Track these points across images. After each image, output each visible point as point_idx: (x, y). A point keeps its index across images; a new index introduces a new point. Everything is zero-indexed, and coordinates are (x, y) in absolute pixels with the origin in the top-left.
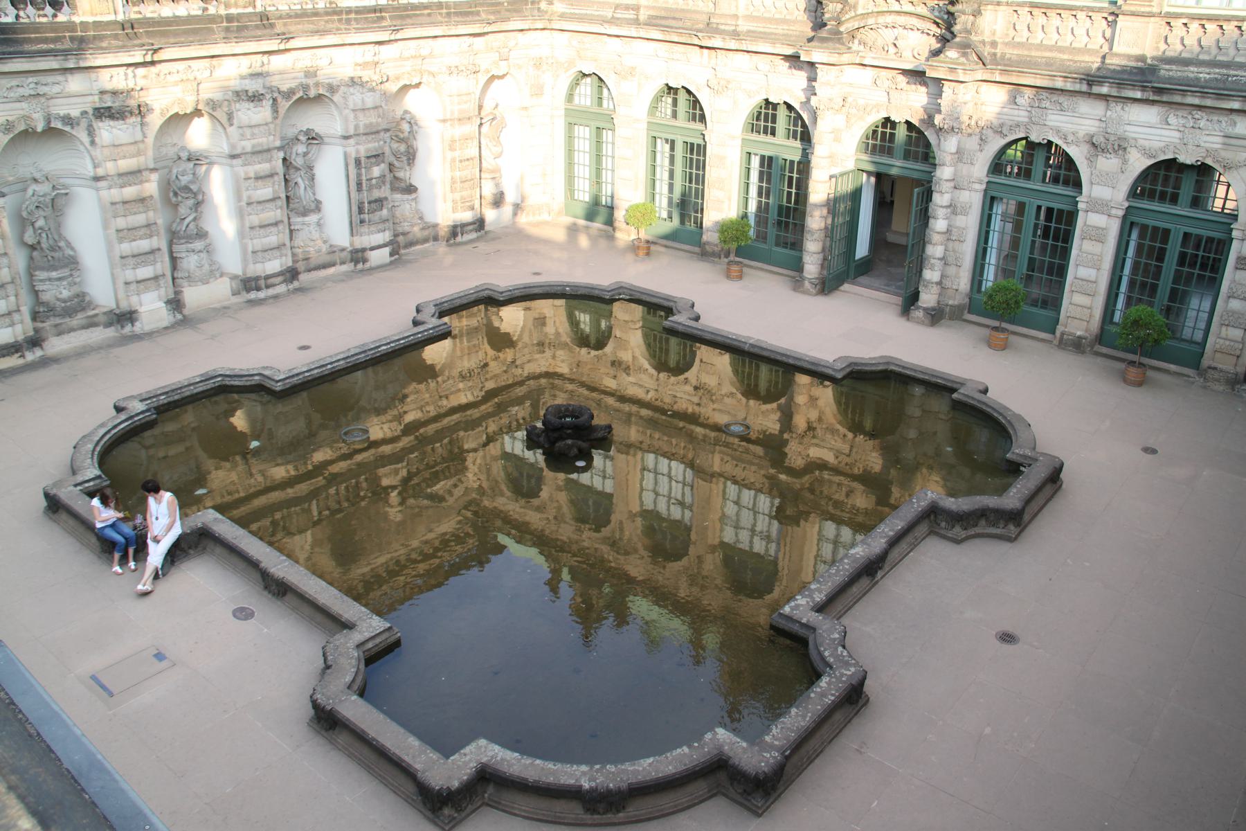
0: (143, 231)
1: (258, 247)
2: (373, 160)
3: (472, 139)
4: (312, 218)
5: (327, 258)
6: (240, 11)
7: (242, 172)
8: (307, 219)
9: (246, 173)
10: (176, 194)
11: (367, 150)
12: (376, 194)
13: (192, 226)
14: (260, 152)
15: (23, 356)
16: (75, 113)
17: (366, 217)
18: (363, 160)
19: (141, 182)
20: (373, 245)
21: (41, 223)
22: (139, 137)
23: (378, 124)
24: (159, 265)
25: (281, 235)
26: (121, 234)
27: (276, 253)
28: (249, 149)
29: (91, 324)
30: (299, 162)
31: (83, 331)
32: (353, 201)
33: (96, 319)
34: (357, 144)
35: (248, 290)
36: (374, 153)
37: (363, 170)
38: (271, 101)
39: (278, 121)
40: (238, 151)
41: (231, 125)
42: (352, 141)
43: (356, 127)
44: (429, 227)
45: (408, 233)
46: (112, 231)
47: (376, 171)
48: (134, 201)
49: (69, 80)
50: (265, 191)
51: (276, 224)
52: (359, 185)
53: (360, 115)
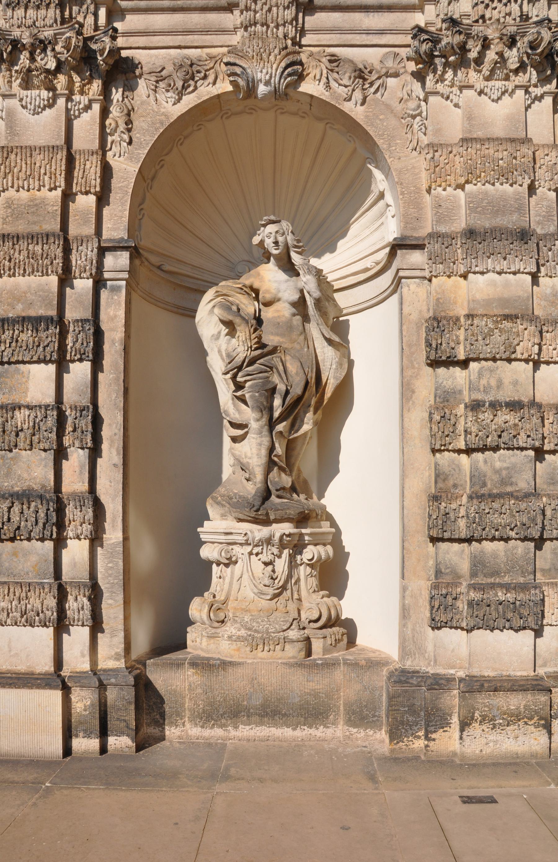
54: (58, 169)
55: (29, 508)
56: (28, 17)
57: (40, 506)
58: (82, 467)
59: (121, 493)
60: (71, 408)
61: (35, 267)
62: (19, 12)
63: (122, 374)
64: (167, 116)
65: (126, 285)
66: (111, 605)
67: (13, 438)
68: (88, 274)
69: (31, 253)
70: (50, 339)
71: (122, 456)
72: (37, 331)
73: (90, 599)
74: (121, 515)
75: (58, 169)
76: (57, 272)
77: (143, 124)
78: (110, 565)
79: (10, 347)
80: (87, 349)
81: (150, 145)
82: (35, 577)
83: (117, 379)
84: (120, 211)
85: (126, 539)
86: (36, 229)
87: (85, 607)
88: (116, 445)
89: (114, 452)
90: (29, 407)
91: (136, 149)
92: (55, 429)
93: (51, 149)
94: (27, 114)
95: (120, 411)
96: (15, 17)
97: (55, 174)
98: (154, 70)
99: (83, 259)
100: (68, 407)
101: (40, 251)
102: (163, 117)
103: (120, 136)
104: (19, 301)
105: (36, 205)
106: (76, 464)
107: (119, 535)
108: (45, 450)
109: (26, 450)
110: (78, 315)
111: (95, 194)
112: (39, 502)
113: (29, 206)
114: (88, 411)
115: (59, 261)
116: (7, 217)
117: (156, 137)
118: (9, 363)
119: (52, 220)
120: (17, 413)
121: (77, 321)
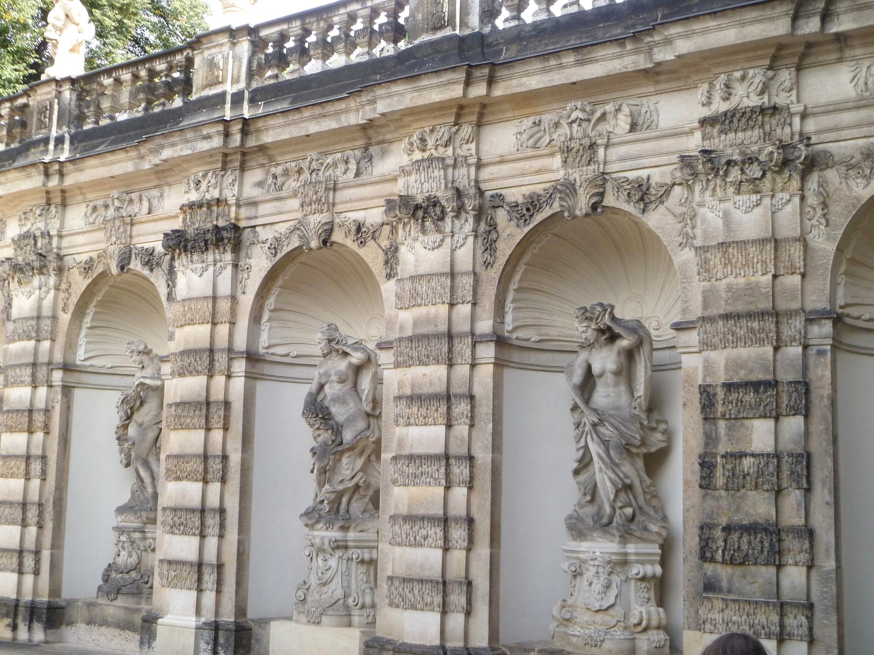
2: (750, 397)
6: (425, 38)
11: (733, 365)
14: (427, 337)
18: (721, 393)
34: (706, 345)
41: (389, 276)
43: (708, 298)
48: (190, 403)
49: (165, 195)
54: (768, 258)
55: (755, 538)
56: (737, 138)
57: (765, 537)
58: (799, 504)
59: (833, 527)
60: (788, 455)
61: (754, 340)
62: (730, 135)
63: (831, 426)
64: (858, 200)
65: (831, 349)
66: (826, 624)
67: (741, 481)
68: (798, 343)
69: (749, 328)
70: (769, 400)
71: (833, 496)
72: (758, 392)
73: (807, 617)
74: (834, 546)
75: (768, 258)
76: (772, 344)
77: (837, 208)
78: (825, 589)
79: (736, 406)
80: (800, 406)
81: (845, 226)
82: (761, 597)
83: (827, 429)
84: (822, 285)
85: (839, 567)
86: (752, 308)
87: (804, 625)
88: (828, 486)
89: (826, 492)
90: (753, 455)
91: (833, 230)
92: (776, 473)
93: (761, 242)
94: (740, 213)
95: (830, 457)
96: (728, 140)
97: (766, 263)
98: (845, 160)
99: (793, 331)
100: (785, 454)
101: (757, 326)
102: (854, 201)
103: (818, 221)
104: (741, 368)
105: (751, 288)
106: (794, 502)
107: (831, 564)
108: (767, 491)
109: (751, 490)
110: (791, 377)
111: (800, 274)
112: (764, 534)
113: (746, 289)
114: (803, 458)
115: (773, 335)
116: (729, 299)
117: (850, 218)
118: (736, 419)
119: (766, 300)
120: (744, 460)
121: (791, 383)
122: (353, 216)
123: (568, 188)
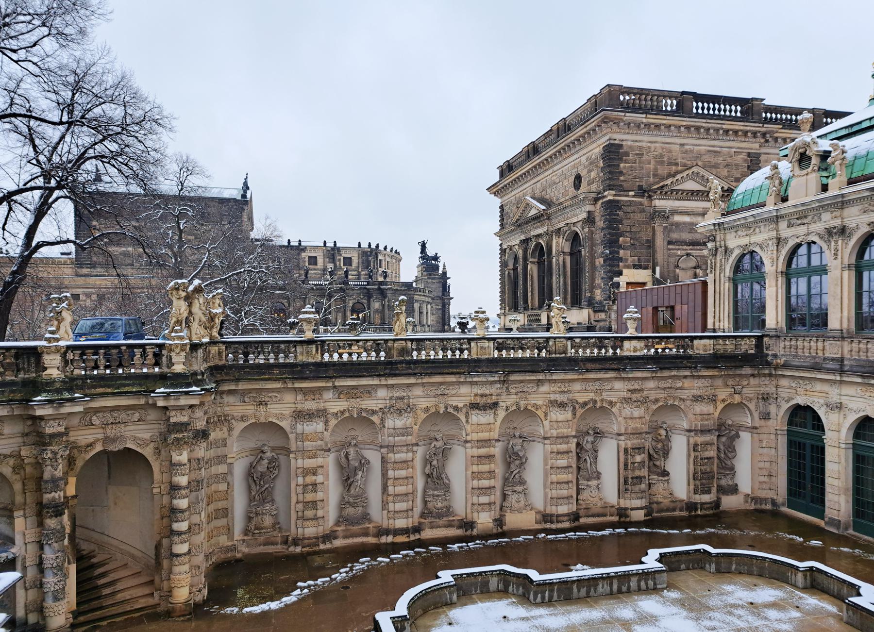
0: (486, 475)
1: (555, 495)
2: (637, 451)
3: (712, 444)
4: (594, 483)
5: (601, 511)
7: (548, 447)
8: (590, 483)
9: (552, 449)
10: (510, 457)
11: (633, 444)
12: (637, 473)
13: (517, 476)
15: (409, 537)
16: (460, 405)
17: (630, 487)
18: (629, 450)
19: (490, 447)
20: (633, 506)
21: (435, 463)
22: (492, 421)
23: (642, 428)
24: (493, 497)
25: (570, 490)
26: (474, 475)
27: (566, 501)
28: (555, 435)
29: (449, 525)
30: (589, 446)
31: (445, 529)
32: (621, 476)
33: (453, 523)
35: (546, 522)
36: (638, 446)
37: (629, 457)
38: (572, 408)
39: (575, 420)
40: (549, 435)
41: (546, 420)
42: (622, 437)
43: (626, 429)
44: (676, 501)
45: (661, 502)
46: (469, 473)
47: (638, 458)
50: (563, 462)
51: (567, 483)
52: (626, 465)
53: (628, 420)
122: (533, 402)
123: (595, 402)
